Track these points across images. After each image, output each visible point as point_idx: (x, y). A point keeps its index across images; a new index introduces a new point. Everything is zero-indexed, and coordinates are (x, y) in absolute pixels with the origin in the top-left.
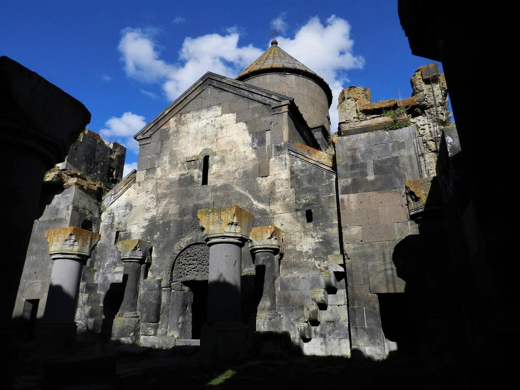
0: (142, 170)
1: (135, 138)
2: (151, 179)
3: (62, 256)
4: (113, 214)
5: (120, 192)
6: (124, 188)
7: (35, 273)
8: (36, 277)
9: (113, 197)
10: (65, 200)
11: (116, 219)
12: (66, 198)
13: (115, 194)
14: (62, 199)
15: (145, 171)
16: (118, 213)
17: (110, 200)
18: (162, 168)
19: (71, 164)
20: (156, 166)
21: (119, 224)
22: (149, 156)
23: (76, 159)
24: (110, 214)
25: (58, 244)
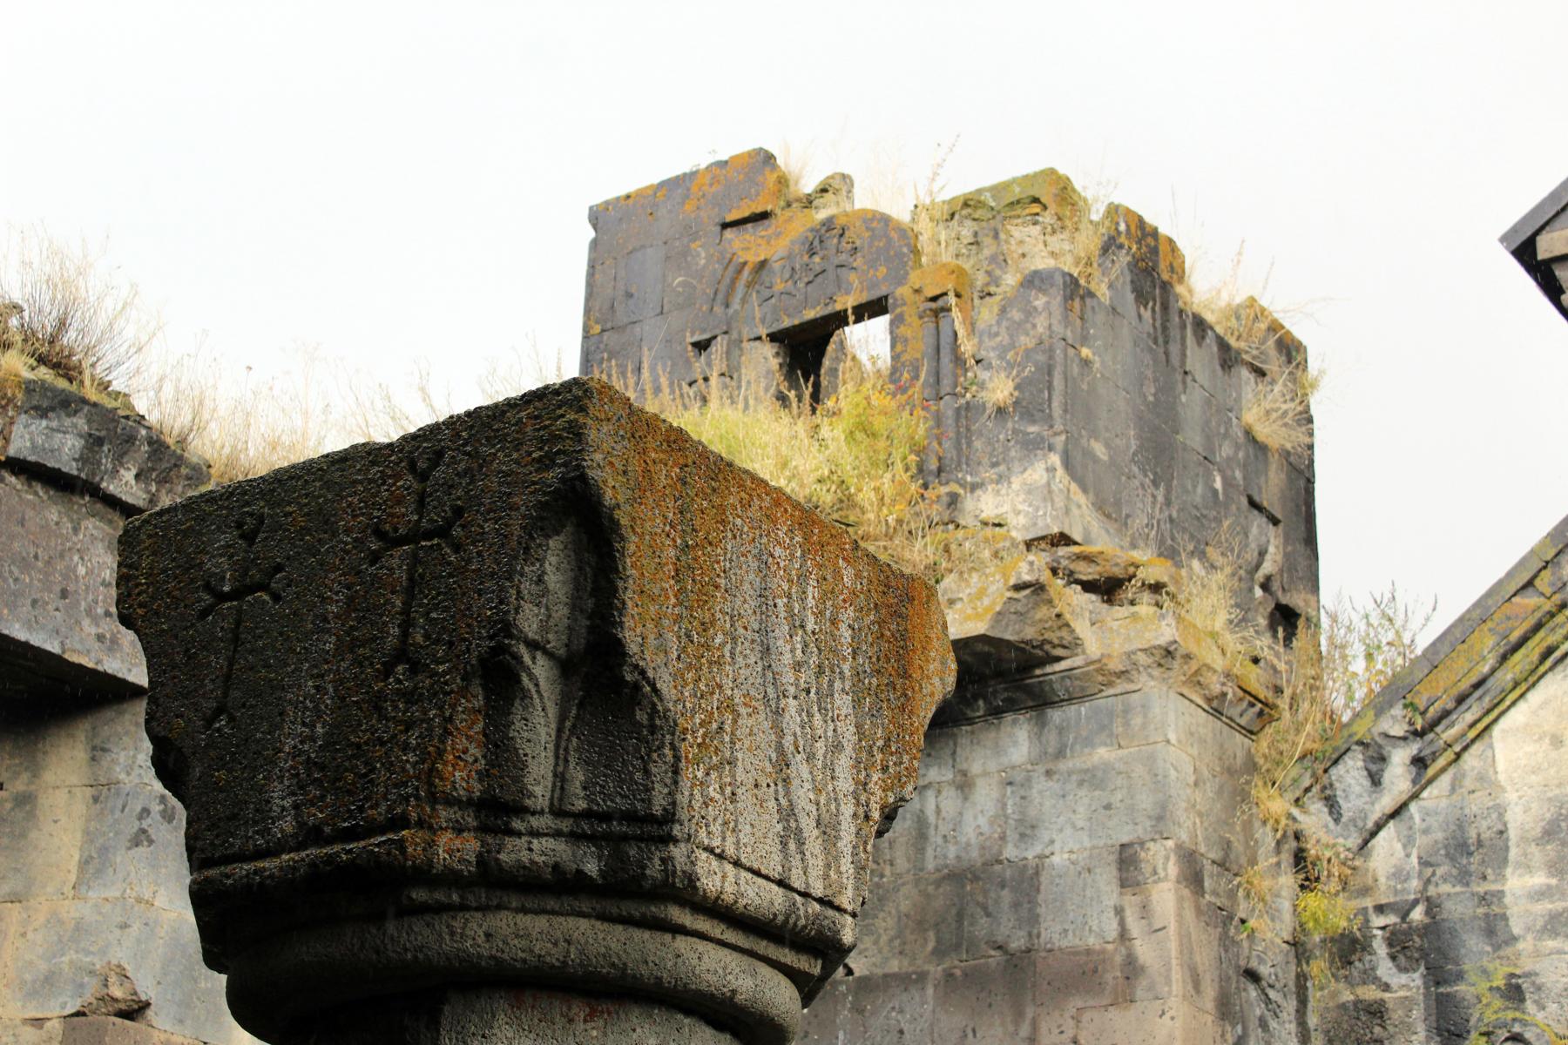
1: (1525, 252)
5: (1469, 717)
10: (1084, 800)
12: (1093, 779)
14: (1040, 784)
19: (1085, 490)
23: (1099, 449)
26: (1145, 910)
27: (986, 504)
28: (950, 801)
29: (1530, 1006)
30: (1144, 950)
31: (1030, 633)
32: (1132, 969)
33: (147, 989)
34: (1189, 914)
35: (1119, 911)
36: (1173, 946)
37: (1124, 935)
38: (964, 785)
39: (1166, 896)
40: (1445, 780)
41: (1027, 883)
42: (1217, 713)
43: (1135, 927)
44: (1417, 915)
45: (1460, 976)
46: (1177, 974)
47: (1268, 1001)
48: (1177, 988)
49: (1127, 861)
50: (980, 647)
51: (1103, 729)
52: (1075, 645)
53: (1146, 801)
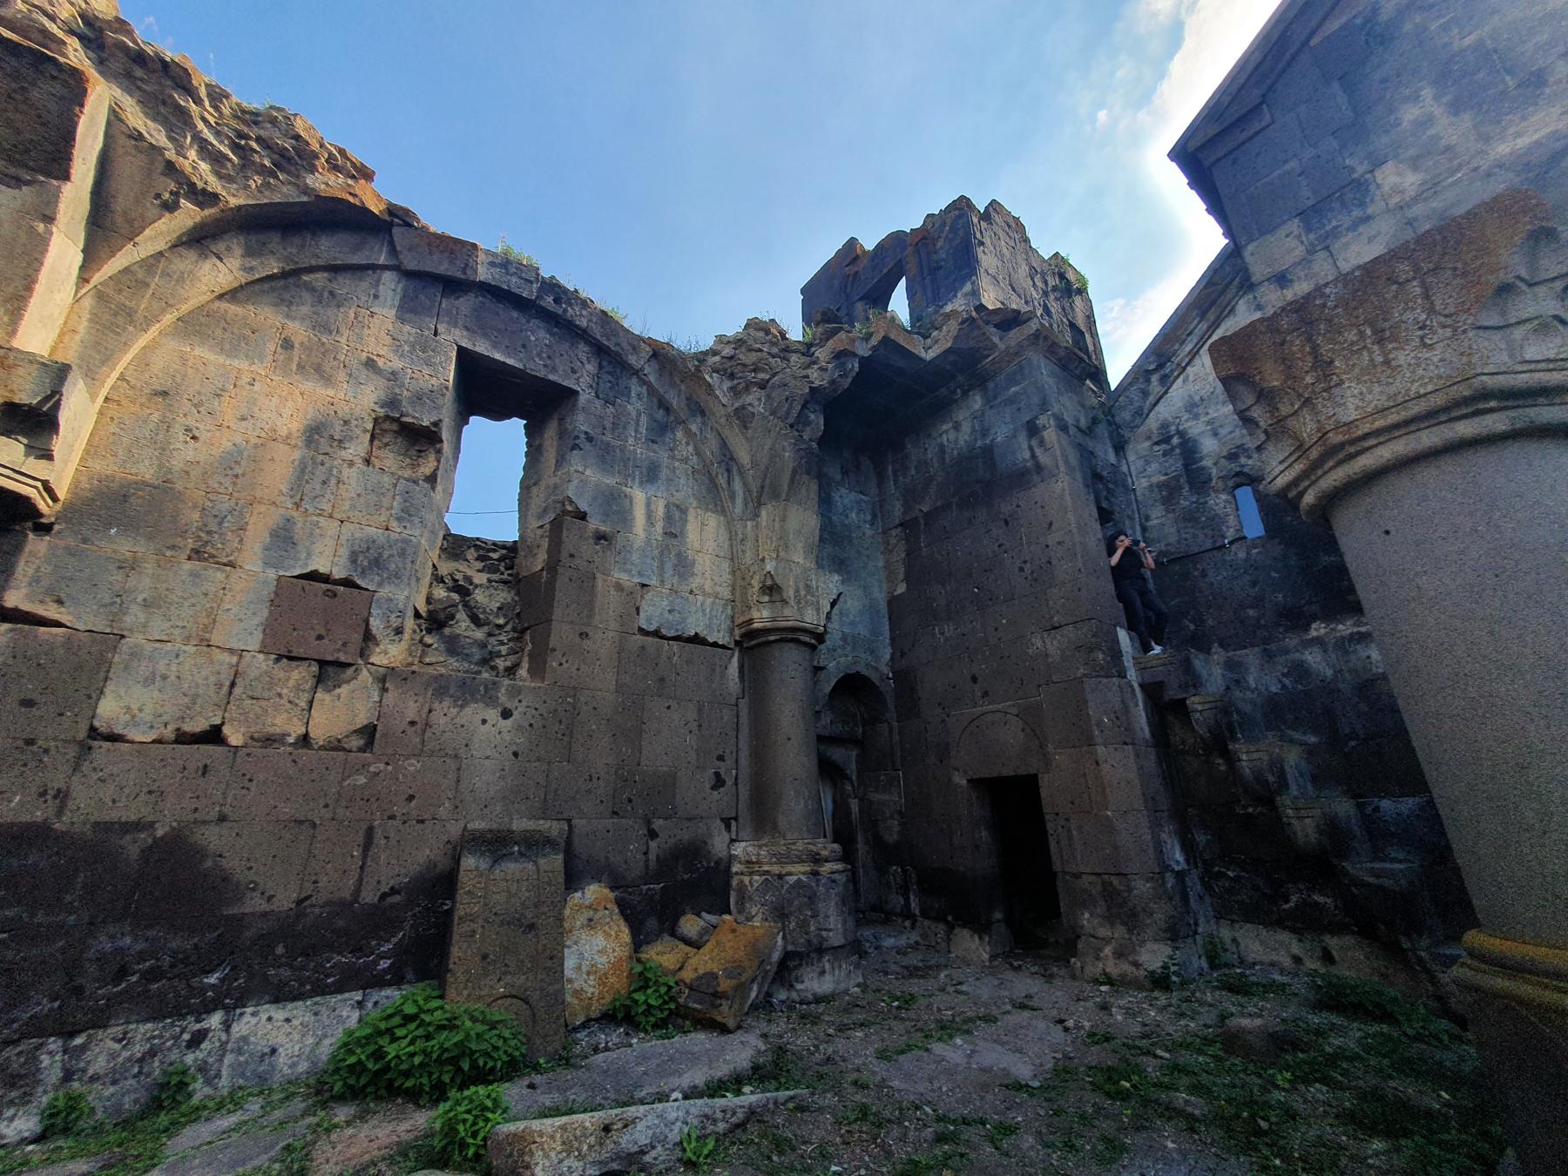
0: (1267, 229)
2: (1354, 227)
3: (1497, 422)
4: (1181, 434)
5: (1188, 348)
6: (1204, 326)
7: (974, 679)
8: (986, 694)
9: (1155, 378)
11: (1209, 446)
12: (1011, 401)
13: (1161, 366)
15: (1295, 225)
16: (1208, 423)
17: (1145, 394)
18: (1412, 152)
20: (1361, 169)
21: (1232, 457)
22: (1293, 164)
24: (1166, 440)
25: (1402, 358)
26: (1042, 443)
27: (948, 308)
28: (952, 435)
29: (1243, 460)
30: (1043, 458)
31: (972, 343)
32: (1039, 468)
33: (583, 506)
34: (1064, 443)
35: (1031, 448)
36: (1058, 453)
37: (1033, 456)
38: (957, 427)
39: (1050, 435)
40: (1180, 380)
41: (988, 452)
42: (1064, 367)
43: (1038, 452)
44: (1175, 441)
45: (1202, 459)
46: (1061, 463)
47: (1108, 489)
48: (1062, 469)
49: (1033, 430)
50: (952, 358)
51: (1013, 381)
52: (995, 346)
53: (1036, 400)
